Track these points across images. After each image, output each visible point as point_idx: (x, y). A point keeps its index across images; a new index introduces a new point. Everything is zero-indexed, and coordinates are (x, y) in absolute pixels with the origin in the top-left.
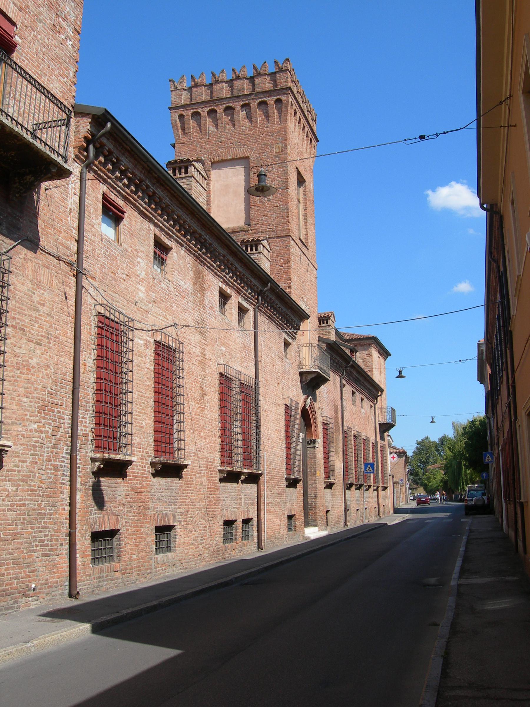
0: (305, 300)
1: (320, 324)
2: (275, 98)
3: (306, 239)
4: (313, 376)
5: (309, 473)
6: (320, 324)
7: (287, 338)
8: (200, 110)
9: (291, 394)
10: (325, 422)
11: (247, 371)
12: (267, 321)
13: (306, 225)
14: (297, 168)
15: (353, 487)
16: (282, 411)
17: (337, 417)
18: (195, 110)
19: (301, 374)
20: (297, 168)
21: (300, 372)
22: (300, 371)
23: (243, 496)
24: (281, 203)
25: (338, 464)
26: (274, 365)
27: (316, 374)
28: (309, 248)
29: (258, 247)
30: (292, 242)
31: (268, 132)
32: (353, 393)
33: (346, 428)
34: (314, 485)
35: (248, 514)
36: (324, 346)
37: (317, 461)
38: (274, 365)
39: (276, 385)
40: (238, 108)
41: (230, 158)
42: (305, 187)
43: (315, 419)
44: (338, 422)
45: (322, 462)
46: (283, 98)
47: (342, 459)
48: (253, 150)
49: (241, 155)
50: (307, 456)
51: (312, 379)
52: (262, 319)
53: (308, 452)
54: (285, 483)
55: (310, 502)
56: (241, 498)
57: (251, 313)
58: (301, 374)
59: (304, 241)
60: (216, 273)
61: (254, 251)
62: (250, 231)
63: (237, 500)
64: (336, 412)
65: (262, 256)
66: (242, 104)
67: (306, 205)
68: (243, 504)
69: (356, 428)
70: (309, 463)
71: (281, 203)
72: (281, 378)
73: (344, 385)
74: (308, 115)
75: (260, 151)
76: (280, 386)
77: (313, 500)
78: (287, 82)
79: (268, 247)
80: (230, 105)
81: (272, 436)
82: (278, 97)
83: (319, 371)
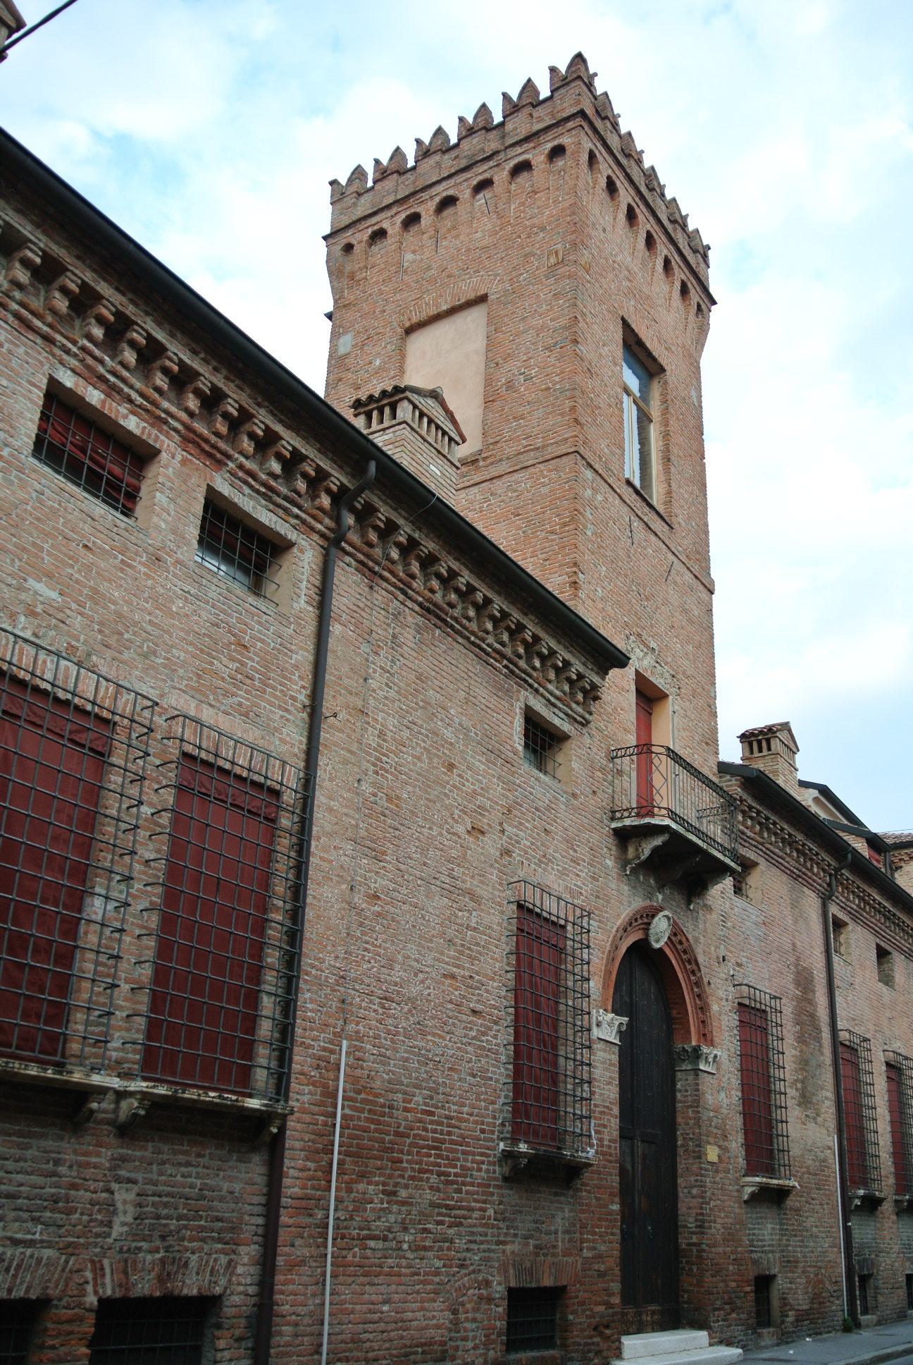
0: (653, 645)
1: (752, 753)
2: (549, 146)
3: (668, 502)
4: (658, 841)
5: (680, 1151)
6: (752, 753)
7: (538, 705)
8: (385, 225)
9: (552, 880)
10: (746, 1002)
11: (263, 737)
12: (412, 618)
13: (667, 471)
14: (623, 319)
15: (888, 1207)
16: (496, 921)
17: (805, 998)
18: (376, 228)
19: (624, 837)
20: (623, 319)
21: (614, 830)
22: (614, 825)
23: (124, 1197)
24: (557, 379)
25: (810, 1134)
26: (451, 766)
27: (665, 837)
28: (676, 526)
29: (398, 411)
30: (589, 474)
31: (533, 226)
32: (882, 954)
33: (844, 1036)
34: (695, 1191)
35: (161, 1280)
36: (733, 786)
37: (706, 1114)
38: (451, 766)
39: (461, 829)
40: (465, 193)
41: (445, 308)
42: (666, 383)
43: (698, 984)
44: (813, 1016)
45: (736, 1122)
46: (566, 140)
47: (832, 1124)
48: (496, 275)
49: (471, 296)
50: (674, 1097)
51: (655, 851)
52: (348, 583)
53: (679, 1086)
54: (487, 1170)
55: (683, 1242)
56: (110, 1208)
57: (304, 559)
58: (624, 837)
59: (661, 509)
60: (17, 316)
61: (386, 424)
62: (481, 463)
63: (69, 1212)
64: (804, 981)
65: (407, 432)
66: (475, 183)
67: (667, 425)
68: (117, 1230)
69: (897, 1045)
70: (679, 1120)
71: (557, 379)
72: (496, 816)
73: (839, 925)
74: (675, 230)
75: (514, 274)
76: (491, 845)
77: (694, 1240)
78: (578, 102)
79: (448, 426)
80: (450, 192)
81: (414, 990)
82: (556, 143)
83: (674, 826)
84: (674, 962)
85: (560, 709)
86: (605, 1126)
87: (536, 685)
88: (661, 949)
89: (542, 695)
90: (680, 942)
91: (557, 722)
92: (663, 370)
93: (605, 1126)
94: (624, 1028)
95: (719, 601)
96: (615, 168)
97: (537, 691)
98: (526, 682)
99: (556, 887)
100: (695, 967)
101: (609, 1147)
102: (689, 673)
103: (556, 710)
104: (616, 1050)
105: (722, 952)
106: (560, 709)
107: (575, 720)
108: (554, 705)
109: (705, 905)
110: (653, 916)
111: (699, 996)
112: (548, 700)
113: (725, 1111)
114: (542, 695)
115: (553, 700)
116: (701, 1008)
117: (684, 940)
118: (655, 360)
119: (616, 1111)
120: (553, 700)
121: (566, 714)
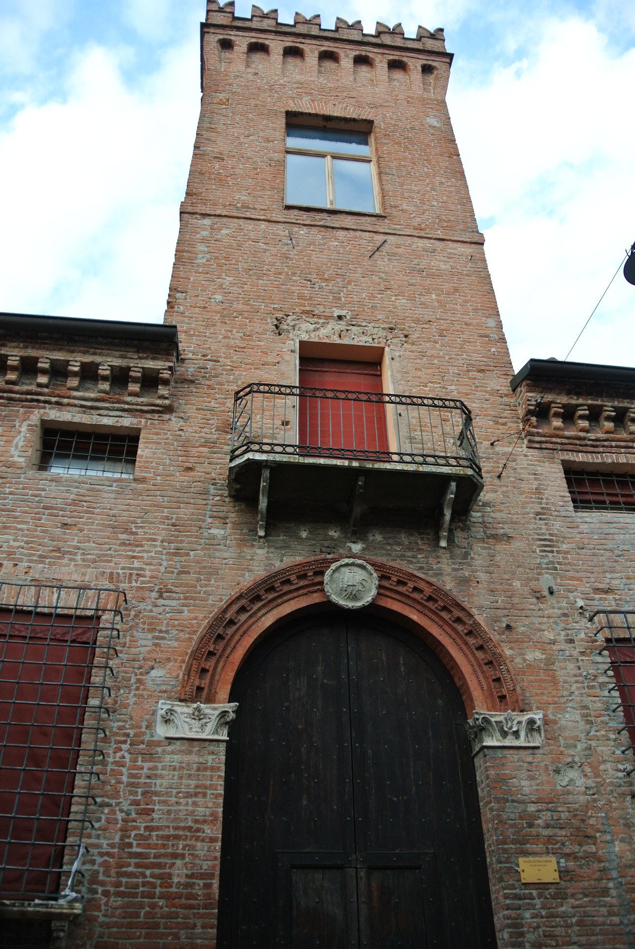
84: (415, 617)
85: (107, 409)
86: (175, 856)
87: (54, 399)
88: (373, 605)
89: (69, 405)
90: (416, 589)
91: (106, 421)
92: (371, 123)
93: (175, 856)
94: (232, 716)
95: (488, 248)
96: (246, 34)
97: (57, 403)
98: (38, 401)
99: (75, 577)
100: (457, 613)
101: (187, 885)
102: (427, 318)
103: (101, 412)
104: (222, 748)
105: (546, 580)
106: (107, 409)
107: (141, 411)
108: (97, 408)
109: (495, 537)
110: (322, 573)
111: (480, 648)
112: (82, 406)
113: (583, 799)
114: (69, 405)
115: (89, 404)
116: (490, 663)
117: (422, 585)
118: (354, 120)
119: (215, 831)
120: (89, 404)
121: (124, 410)
